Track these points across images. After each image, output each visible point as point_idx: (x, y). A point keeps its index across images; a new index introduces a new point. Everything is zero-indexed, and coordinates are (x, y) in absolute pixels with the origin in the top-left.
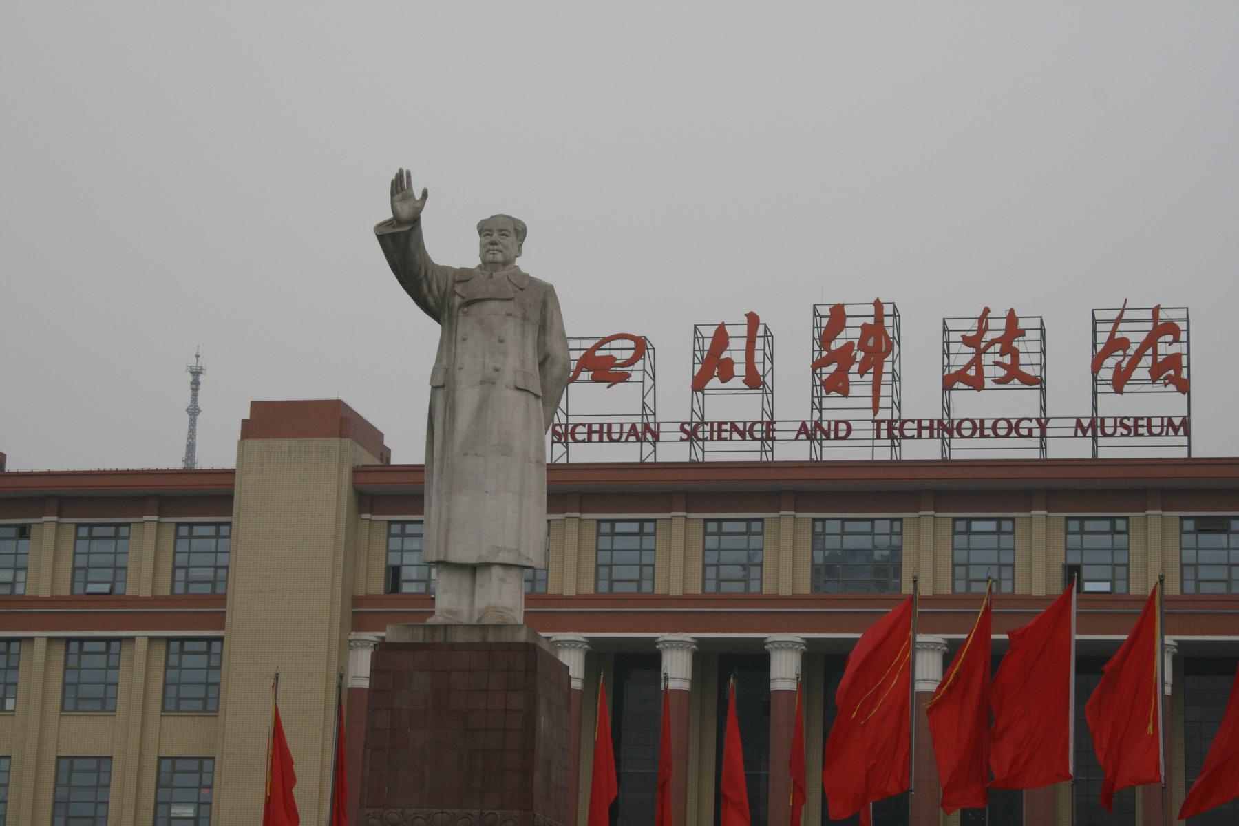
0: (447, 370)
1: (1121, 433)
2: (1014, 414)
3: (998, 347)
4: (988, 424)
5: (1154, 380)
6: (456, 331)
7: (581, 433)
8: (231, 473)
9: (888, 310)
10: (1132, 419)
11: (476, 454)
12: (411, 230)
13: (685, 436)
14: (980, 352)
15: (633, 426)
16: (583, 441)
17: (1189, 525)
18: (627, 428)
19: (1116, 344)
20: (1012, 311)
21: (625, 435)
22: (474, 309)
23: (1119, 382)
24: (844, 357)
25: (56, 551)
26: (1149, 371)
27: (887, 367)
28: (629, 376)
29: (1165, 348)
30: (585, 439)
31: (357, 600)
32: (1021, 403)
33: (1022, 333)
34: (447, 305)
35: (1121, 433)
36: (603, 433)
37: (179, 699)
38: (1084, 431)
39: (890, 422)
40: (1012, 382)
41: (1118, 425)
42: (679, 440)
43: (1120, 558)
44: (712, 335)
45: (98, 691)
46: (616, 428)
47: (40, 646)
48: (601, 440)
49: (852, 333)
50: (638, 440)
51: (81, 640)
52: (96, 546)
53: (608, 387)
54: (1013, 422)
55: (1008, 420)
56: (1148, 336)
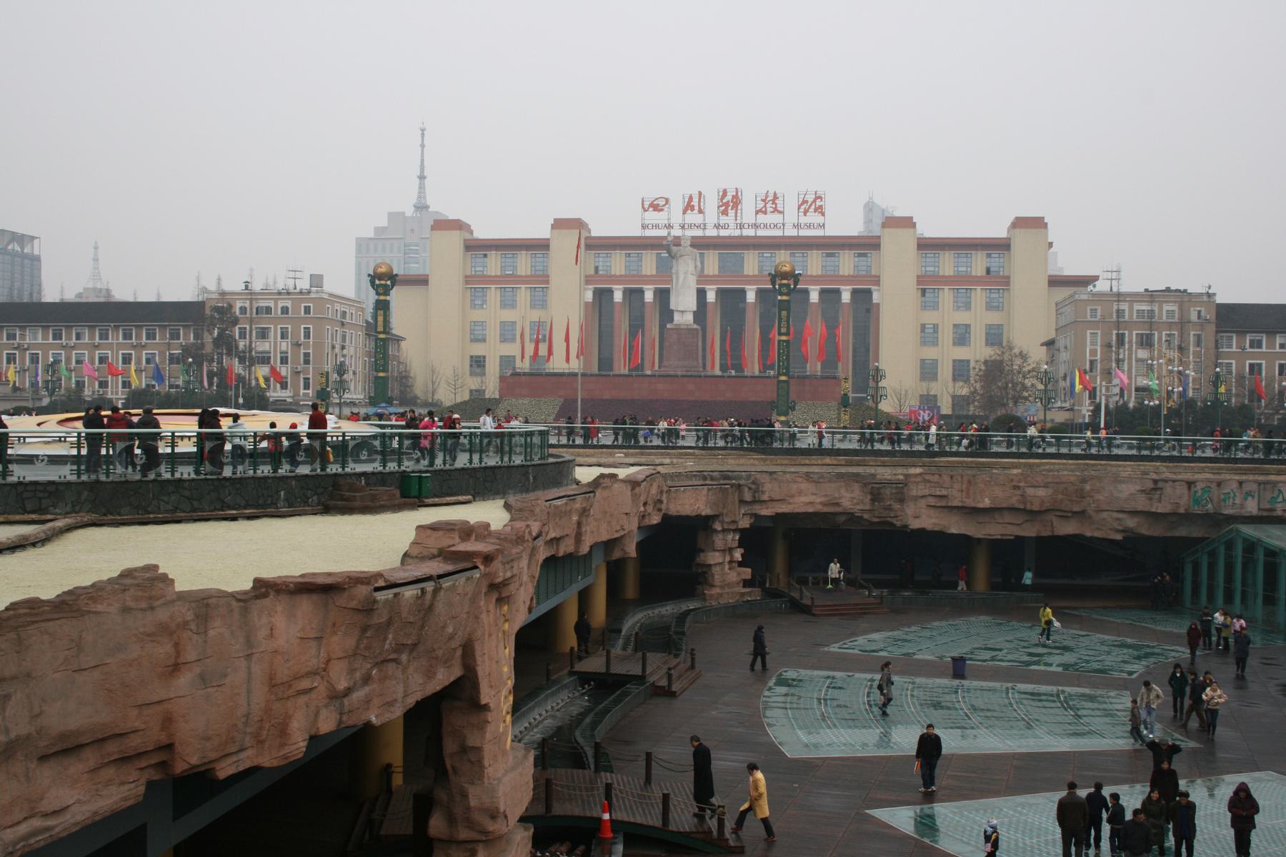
7: (650, 226)
8: (549, 239)
14: (766, 204)
17: (824, 255)
19: (805, 202)
23: (805, 212)
24: (727, 204)
27: (739, 208)
29: (819, 203)
31: (586, 276)
32: (776, 218)
36: (657, 226)
37: (475, 305)
43: (805, 264)
45: (511, 303)
47: (493, 289)
49: (729, 198)
52: (507, 260)
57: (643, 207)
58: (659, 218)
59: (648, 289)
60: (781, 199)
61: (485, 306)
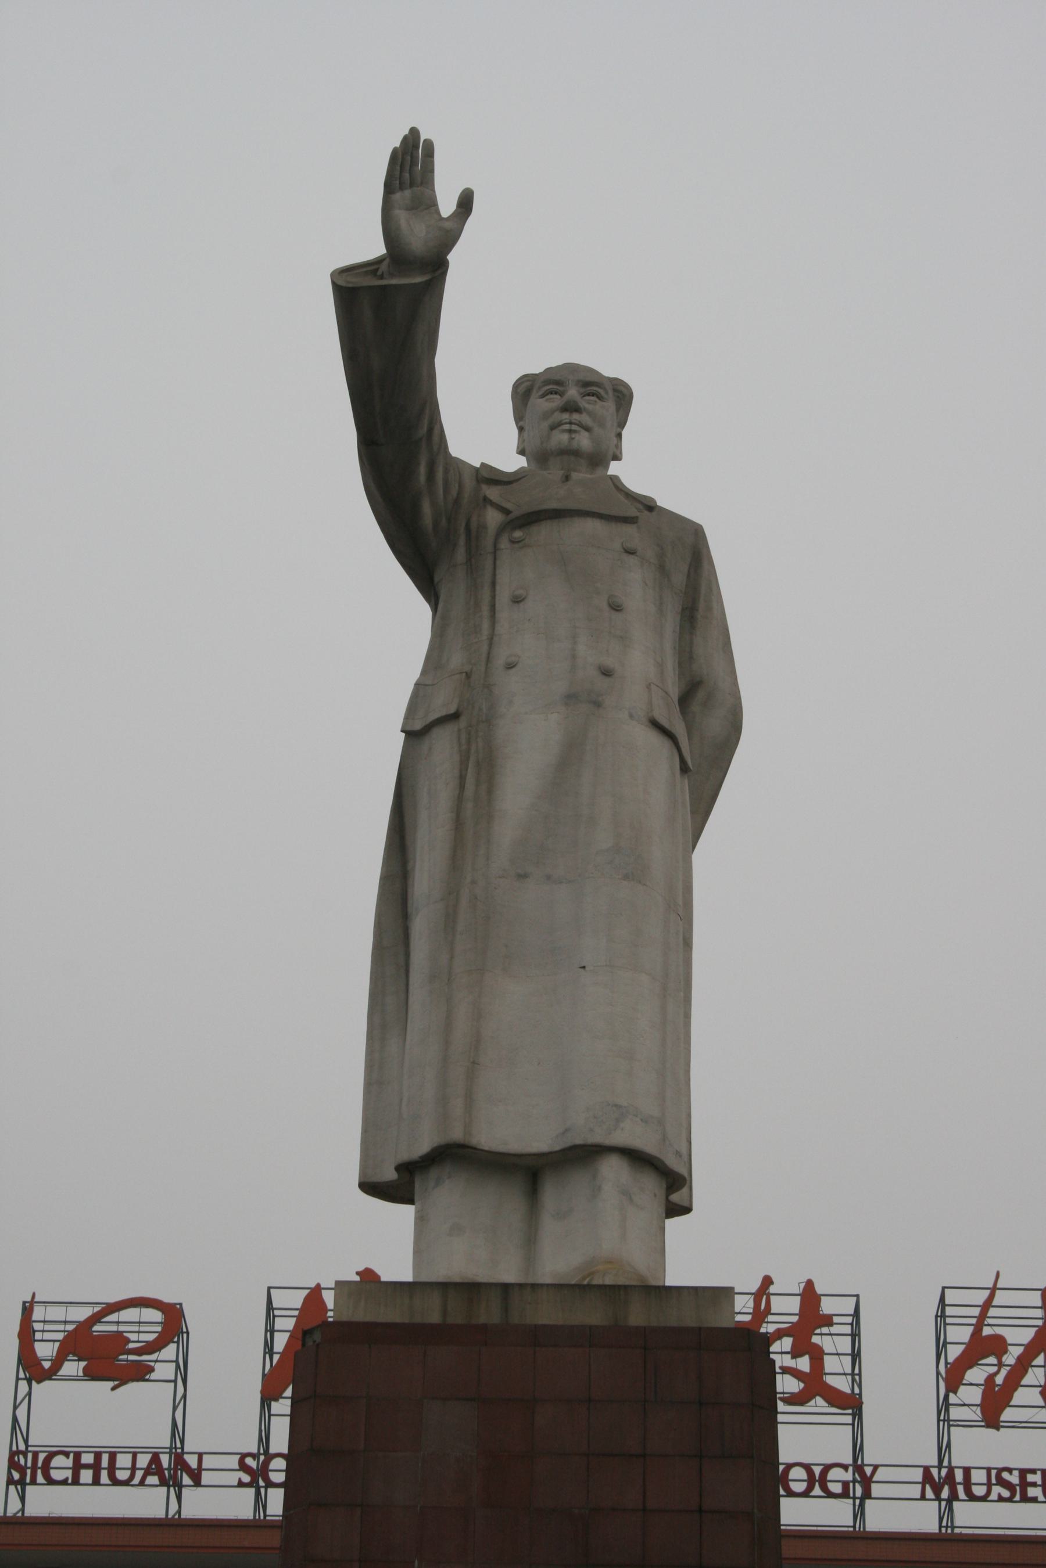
0: (468, 675)
1: (999, 1495)
2: (818, 1457)
3: (787, 1343)
6: (493, 584)
10: (1016, 1473)
11: (548, 877)
12: (431, 280)
13: (246, 1478)
15: (155, 1458)
16: (64, 1482)
18: (143, 1461)
20: (810, 1284)
21: (139, 1474)
22: (543, 532)
26: (1041, 1393)
28: (152, 1370)
30: (67, 1479)
33: (828, 1321)
34: (462, 530)
35: (999, 1495)
38: (937, 1491)
40: (813, 1403)
41: (994, 1481)
42: (236, 1483)
44: (299, 1307)
46: (124, 1461)
48: (96, 1481)
50: (163, 1482)
53: (113, 1389)
54: (817, 1470)
55: (808, 1468)
56: (1037, 1333)
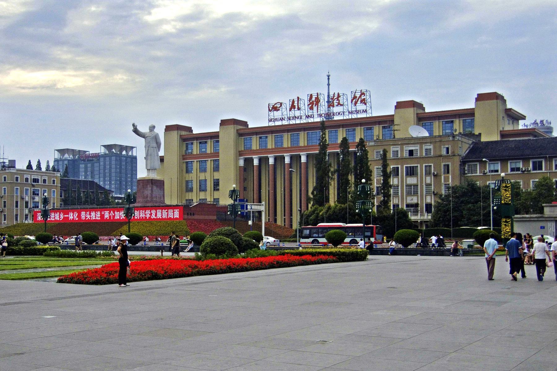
2: (339, 111)
4: (335, 113)
5: (361, 103)
9: (319, 94)
14: (334, 101)
19: (355, 97)
23: (356, 103)
25: (197, 146)
27: (319, 104)
29: (363, 97)
39: (320, 114)
46: (278, 119)
49: (313, 99)
51: (201, 161)
57: (269, 110)
58: (277, 114)
59: (270, 157)
60: (342, 97)
61: (192, 171)
